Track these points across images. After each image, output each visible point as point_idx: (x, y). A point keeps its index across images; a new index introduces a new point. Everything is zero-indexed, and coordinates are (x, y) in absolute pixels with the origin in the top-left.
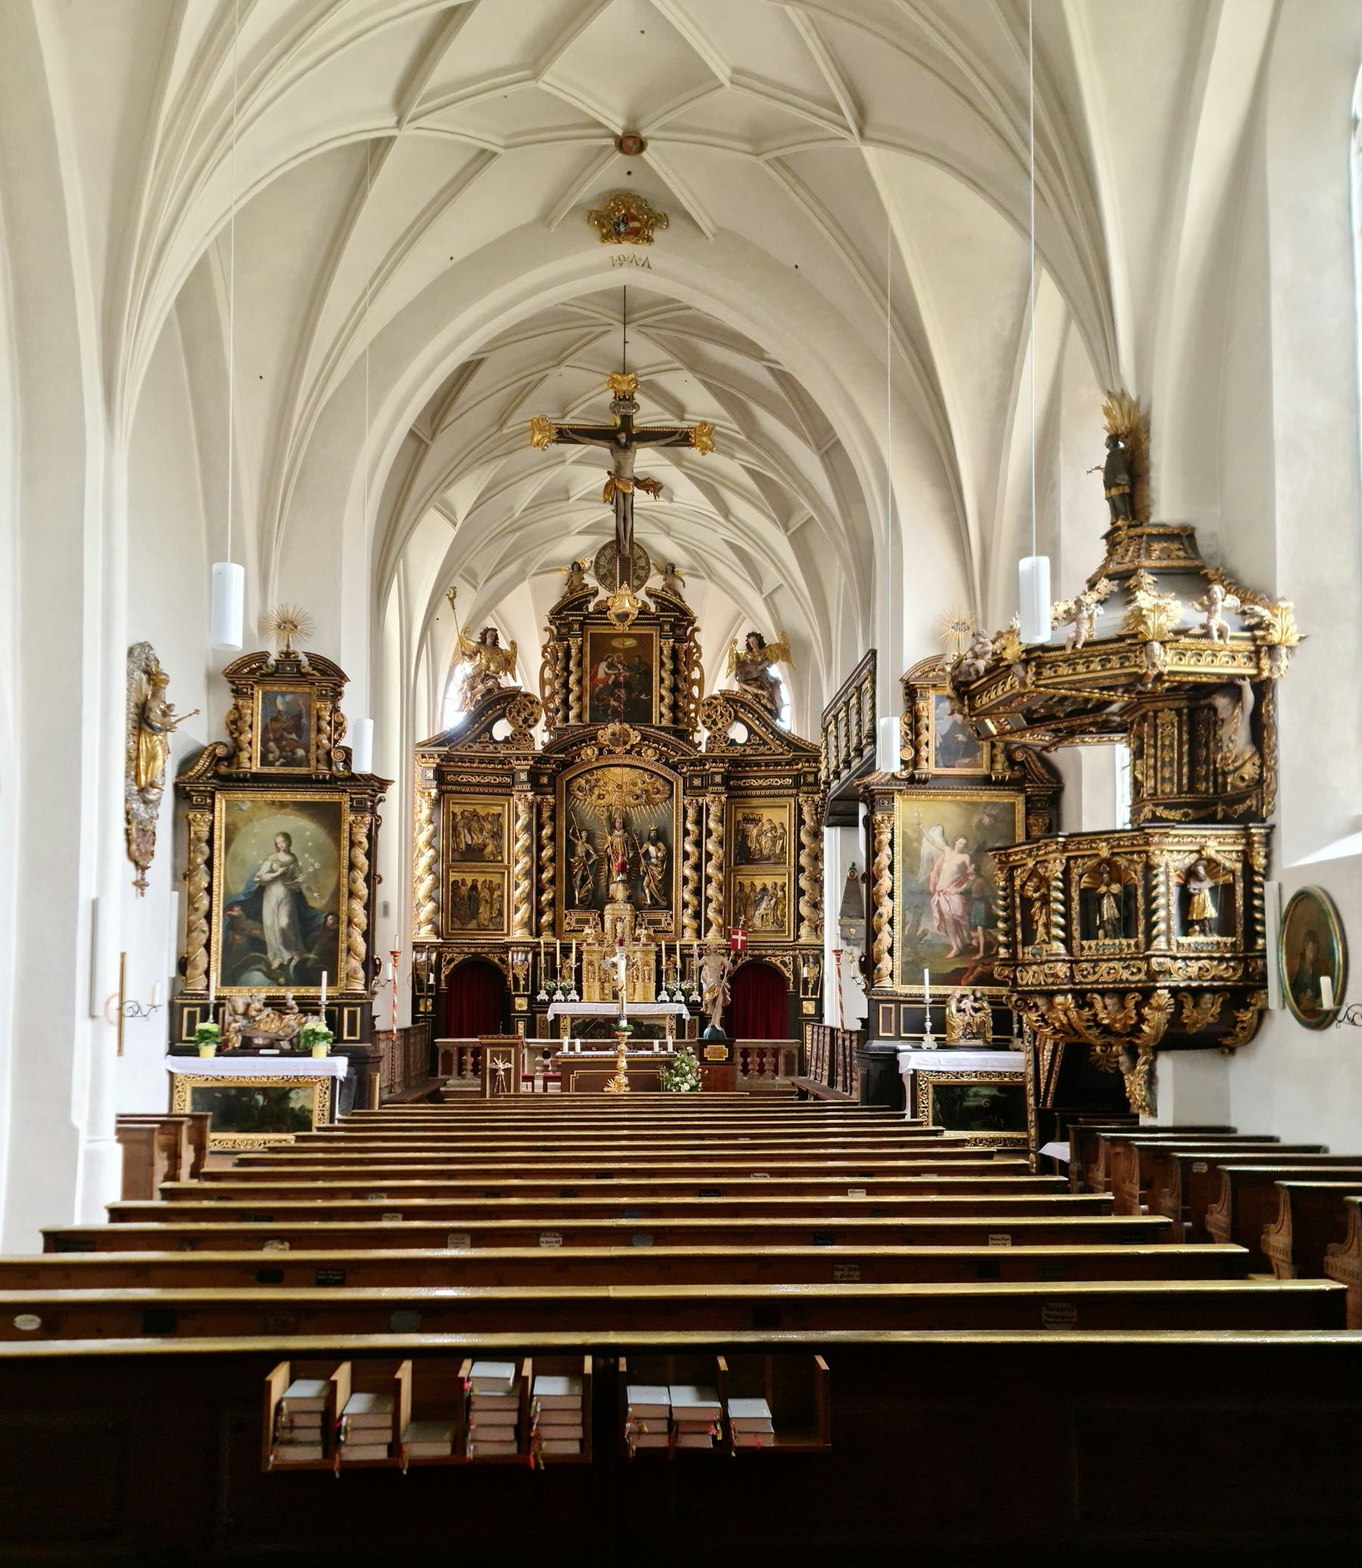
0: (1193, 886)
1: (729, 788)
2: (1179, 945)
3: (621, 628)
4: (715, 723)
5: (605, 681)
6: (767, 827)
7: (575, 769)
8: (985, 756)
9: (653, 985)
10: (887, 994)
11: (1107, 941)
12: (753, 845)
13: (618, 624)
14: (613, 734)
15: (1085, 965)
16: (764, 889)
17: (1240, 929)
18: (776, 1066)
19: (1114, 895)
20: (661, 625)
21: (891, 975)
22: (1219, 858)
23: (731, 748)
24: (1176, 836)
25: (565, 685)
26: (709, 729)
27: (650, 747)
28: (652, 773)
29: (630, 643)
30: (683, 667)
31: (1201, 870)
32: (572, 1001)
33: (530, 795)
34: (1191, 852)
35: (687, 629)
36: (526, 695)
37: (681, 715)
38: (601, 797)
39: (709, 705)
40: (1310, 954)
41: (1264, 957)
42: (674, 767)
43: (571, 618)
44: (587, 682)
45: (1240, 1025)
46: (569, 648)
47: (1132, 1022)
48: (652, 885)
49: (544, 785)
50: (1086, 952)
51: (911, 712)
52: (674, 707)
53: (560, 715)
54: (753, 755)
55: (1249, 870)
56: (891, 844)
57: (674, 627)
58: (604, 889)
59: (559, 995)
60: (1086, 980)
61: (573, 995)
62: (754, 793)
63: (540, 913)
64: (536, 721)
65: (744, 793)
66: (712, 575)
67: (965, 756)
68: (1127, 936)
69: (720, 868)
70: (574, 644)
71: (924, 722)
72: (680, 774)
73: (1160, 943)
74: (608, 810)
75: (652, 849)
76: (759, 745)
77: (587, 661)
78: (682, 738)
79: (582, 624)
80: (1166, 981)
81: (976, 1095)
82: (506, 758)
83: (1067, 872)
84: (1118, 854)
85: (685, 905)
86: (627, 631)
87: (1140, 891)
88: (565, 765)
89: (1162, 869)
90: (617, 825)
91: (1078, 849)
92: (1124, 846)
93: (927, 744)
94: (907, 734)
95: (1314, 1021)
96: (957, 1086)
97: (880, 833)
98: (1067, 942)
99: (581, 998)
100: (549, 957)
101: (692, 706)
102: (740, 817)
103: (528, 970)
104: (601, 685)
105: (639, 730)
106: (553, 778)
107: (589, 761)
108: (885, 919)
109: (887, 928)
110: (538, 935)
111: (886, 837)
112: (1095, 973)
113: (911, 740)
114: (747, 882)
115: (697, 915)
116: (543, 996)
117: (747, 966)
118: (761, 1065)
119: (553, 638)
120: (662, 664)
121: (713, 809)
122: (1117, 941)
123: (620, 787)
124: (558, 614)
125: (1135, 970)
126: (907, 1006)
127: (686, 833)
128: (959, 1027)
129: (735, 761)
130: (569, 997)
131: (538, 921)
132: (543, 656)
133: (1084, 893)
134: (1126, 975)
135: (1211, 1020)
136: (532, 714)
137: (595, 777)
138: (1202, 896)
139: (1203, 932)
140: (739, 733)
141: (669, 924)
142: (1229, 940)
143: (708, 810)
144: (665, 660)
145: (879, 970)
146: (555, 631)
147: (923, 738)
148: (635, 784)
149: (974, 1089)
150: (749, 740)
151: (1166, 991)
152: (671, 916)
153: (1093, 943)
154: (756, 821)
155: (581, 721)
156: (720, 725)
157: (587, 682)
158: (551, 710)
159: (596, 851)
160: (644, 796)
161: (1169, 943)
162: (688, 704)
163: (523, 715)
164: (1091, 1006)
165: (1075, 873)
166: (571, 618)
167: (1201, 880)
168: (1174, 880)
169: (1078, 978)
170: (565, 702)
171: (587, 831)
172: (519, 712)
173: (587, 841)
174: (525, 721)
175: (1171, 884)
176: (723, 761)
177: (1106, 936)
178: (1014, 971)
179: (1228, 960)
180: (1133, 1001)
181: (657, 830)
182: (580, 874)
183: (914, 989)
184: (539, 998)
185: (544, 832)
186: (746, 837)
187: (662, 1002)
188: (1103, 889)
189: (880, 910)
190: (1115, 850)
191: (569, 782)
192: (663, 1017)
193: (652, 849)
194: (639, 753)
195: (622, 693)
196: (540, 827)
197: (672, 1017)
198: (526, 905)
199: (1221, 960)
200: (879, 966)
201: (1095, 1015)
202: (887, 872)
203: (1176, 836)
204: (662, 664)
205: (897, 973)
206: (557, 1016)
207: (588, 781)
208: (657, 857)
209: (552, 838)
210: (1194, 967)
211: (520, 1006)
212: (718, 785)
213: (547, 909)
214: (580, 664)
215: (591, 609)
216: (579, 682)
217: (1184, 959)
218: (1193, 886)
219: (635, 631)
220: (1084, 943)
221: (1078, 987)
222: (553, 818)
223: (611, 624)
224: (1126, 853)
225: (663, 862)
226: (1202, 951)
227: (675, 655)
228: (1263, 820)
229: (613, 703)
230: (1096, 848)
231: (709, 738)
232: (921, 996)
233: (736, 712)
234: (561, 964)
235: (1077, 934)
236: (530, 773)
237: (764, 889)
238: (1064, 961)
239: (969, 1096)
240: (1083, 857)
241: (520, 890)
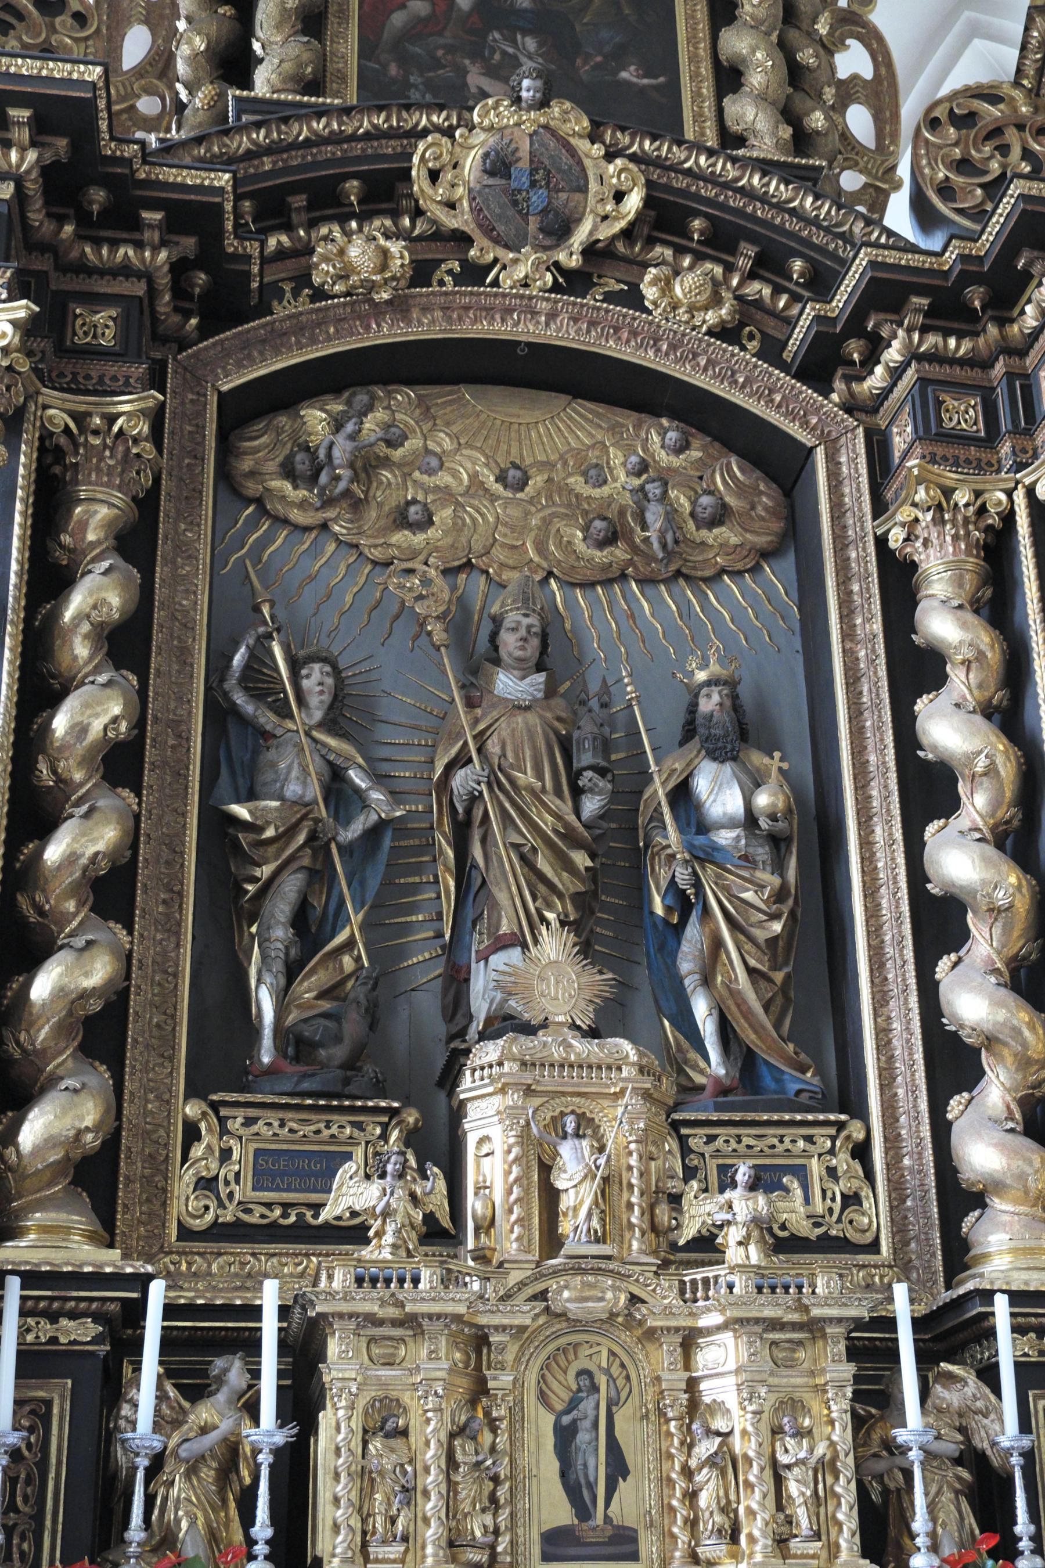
7: (276, 340)
90: (509, 642)
141: (851, 1200)
171: (331, 662)
173: (332, 723)
182: (291, 886)
185: (77, 602)
208: (750, 820)
213: (64, 1059)
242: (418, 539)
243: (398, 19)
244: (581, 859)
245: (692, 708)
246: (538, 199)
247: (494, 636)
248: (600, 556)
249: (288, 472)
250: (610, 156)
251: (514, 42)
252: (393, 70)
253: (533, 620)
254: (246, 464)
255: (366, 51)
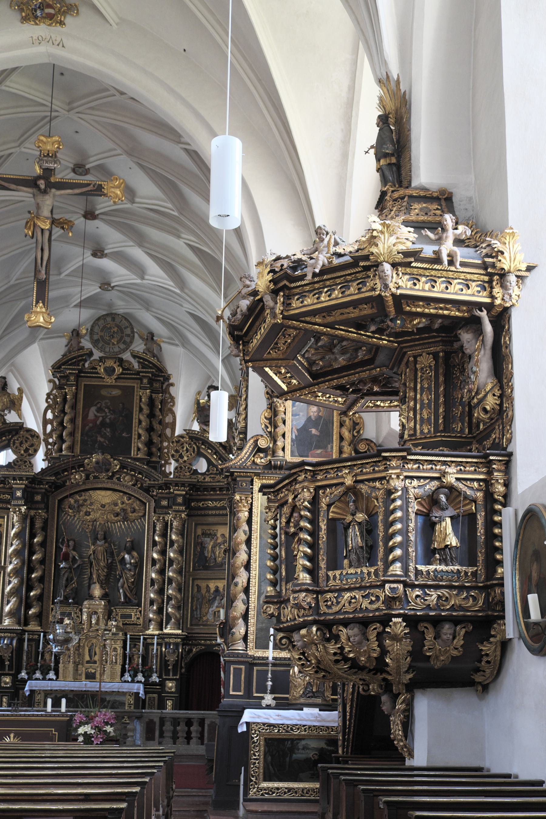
0: (436, 513)
1: (189, 507)
2: (418, 573)
3: (109, 381)
4: (181, 456)
5: (94, 421)
6: (220, 540)
8: (334, 448)
9: (119, 668)
10: (238, 655)
11: (352, 571)
12: (208, 554)
13: (106, 377)
14: (97, 463)
15: (329, 595)
16: (217, 590)
17: (481, 557)
18: (202, 733)
19: (359, 524)
20: (141, 379)
21: (245, 638)
22: (460, 486)
23: (193, 477)
24: (416, 461)
25: (61, 423)
26: (177, 461)
27: (127, 474)
28: (130, 496)
29: (116, 392)
30: (158, 413)
31: (443, 498)
32: (50, 680)
33: (23, 509)
34: (432, 479)
35: (163, 383)
36: (29, 430)
37: (154, 450)
38: (87, 514)
39: (178, 442)
40: (535, 575)
41: (502, 585)
42: (147, 490)
43: (68, 372)
44: (79, 421)
45: (485, 659)
46: (66, 394)
47: (375, 655)
48: (126, 585)
49: (37, 502)
50: (331, 583)
51: (271, 408)
52: (149, 443)
53: (55, 447)
54: (210, 482)
55: (489, 497)
56: (249, 522)
57: (151, 381)
58: (86, 589)
59: (38, 675)
60: (330, 611)
61: (52, 675)
62: (210, 512)
63: (28, 607)
64: (36, 451)
65: (203, 512)
66: (185, 342)
67: (317, 447)
68: (371, 566)
69: (179, 572)
70: (70, 391)
71: (281, 415)
72: (152, 496)
73: (397, 568)
74: (92, 525)
75: (127, 556)
76: (216, 474)
77: (80, 405)
78: (155, 468)
79: (78, 376)
80: (401, 609)
81: (305, 748)
82: (5, 478)
83: (315, 501)
84: (362, 481)
85: (152, 602)
86: (114, 383)
87: (380, 518)
88: (57, 487)
89: (399, 493)
90: (99, 536)
91: (326, 478)
92: (367, 473)
93: (284, 436)
94: (267, 427)
95: (537, 646)
96: (288, 740)
97: (239, 511)
98: (312, 572)
99: (57, 677)
100: (33, 644)
101: (165, 444)
102: (199, 532)
103: (12, 653)
104: (91, 425)
105: (118, 460)
106: (46, 496)
107: (77, 484)
108: (240, 587)
109: (242, 596)
110: (26, 624)
111: (244, 515)
112: (338, 603)
113: (270, 432)
114: (203, 584)
115: (160, 611)
116: (23, 674)
117: (200, 656)
118: (189, 733)
119: (55, 387)
120: (141, 410)
121: (175, 524)
122: (359, 571)
123: (103, 506)
124: (57, 368)
125: (374, 599)
126: (259, 668)
127: (155, 543)
128: (300, 685)
129: (194, 486)
130: (48, 677)
131: (26, 613)
132: (47, 401)
133: (332, 523)
134: (365, 604)
135: (455, 653)
136: (32, 445)
137: (83, 498)
138: (444, 524)
139: (444, 561)
140: (202, 466)
142: (470, 570)
143: (171, 524)
144: (143, 406)
145: (233, 634)
146: (57, 382)
147: (281, 429)
148: (116, 504)
149: (303, 742)
150: (208, 470)
151: (400, 620)
152: (140, 612)
153: (338, 573)
154: (212, 536)
155: (72, 453)
156: (186, 458)
157: (79, 421)
158: (50, 444)
159: (81, 557)
160: (123, 514)
161: (406, 569)
162: (161, 442)
163: (25, 446)
164: (337, 638)
165: (324, 502)
166: (68, 372)
167: (443, 509)
168: (414, 507)
169: (323, 609)
170: (60, 437)
172: (21, 443)
174: (26, 450)
175: (410, 510)
176: (183, 485)
177: (350, 566)
178: (279, 609)
179: (469, 589)
180: (375, 632)
181: (132, 542)
182: (66, 576)
183: (260, 653)
184: (20, 676)
186: (203, 548)
187: (125, 682)
188: (349, 518)
189: (237, 580)
190: (359, 478)
191: (61, 501)
192: (124, 694)
193: (127, 556)
194: (119, 479)
195: (108, 432)
196: (33, 536)
197: (130, 694)
198: (14, 599)
199: (461, 588)
200: (234, 630)
201: (342, 648)
202: (244, 547)
203: (416, 461)
204: (141, 410)
205: (251, 637)
206: (32, 692)
207: (76, 501)
209: (43, 544)
210: (433, 596)
211: (6, 683)
212: (179, 505)
214: (74, 407)
215: (87, 365)
216: (73, 421)
217: (422, 587)
218: (436, 513)
219: (120, 383)
220: (330, 573)
221: (322, 618)
222: (44, 528)
223: (101, 378)
224: (369, 480)
225: (136, 567)
226: (441, 581)
227: (151, 403)
228: (505, 449)
229: (99, 439)
230: (342, 477)
231: (176, 468)
232: (267, 658)
233: (198, 448)
234: (43, 648)
235: (323, 565)
236: (24, 491)
237: (217, 590)
238: (307, 591)
239: (298, 749)
240: (330, 486)
241: (11, 586)
242: (88, 518)
243: (87, 428)
244: (105, 570)
245: (126, 545)
246: (104, 467)
247: (97, 534)
248: (116, 519)
249: (69, 508)
250: (114, 460)
251: (105, 429)
252: (86, 438)
253: (103, 533)
254: (63, 506)
255: (82, 435)
